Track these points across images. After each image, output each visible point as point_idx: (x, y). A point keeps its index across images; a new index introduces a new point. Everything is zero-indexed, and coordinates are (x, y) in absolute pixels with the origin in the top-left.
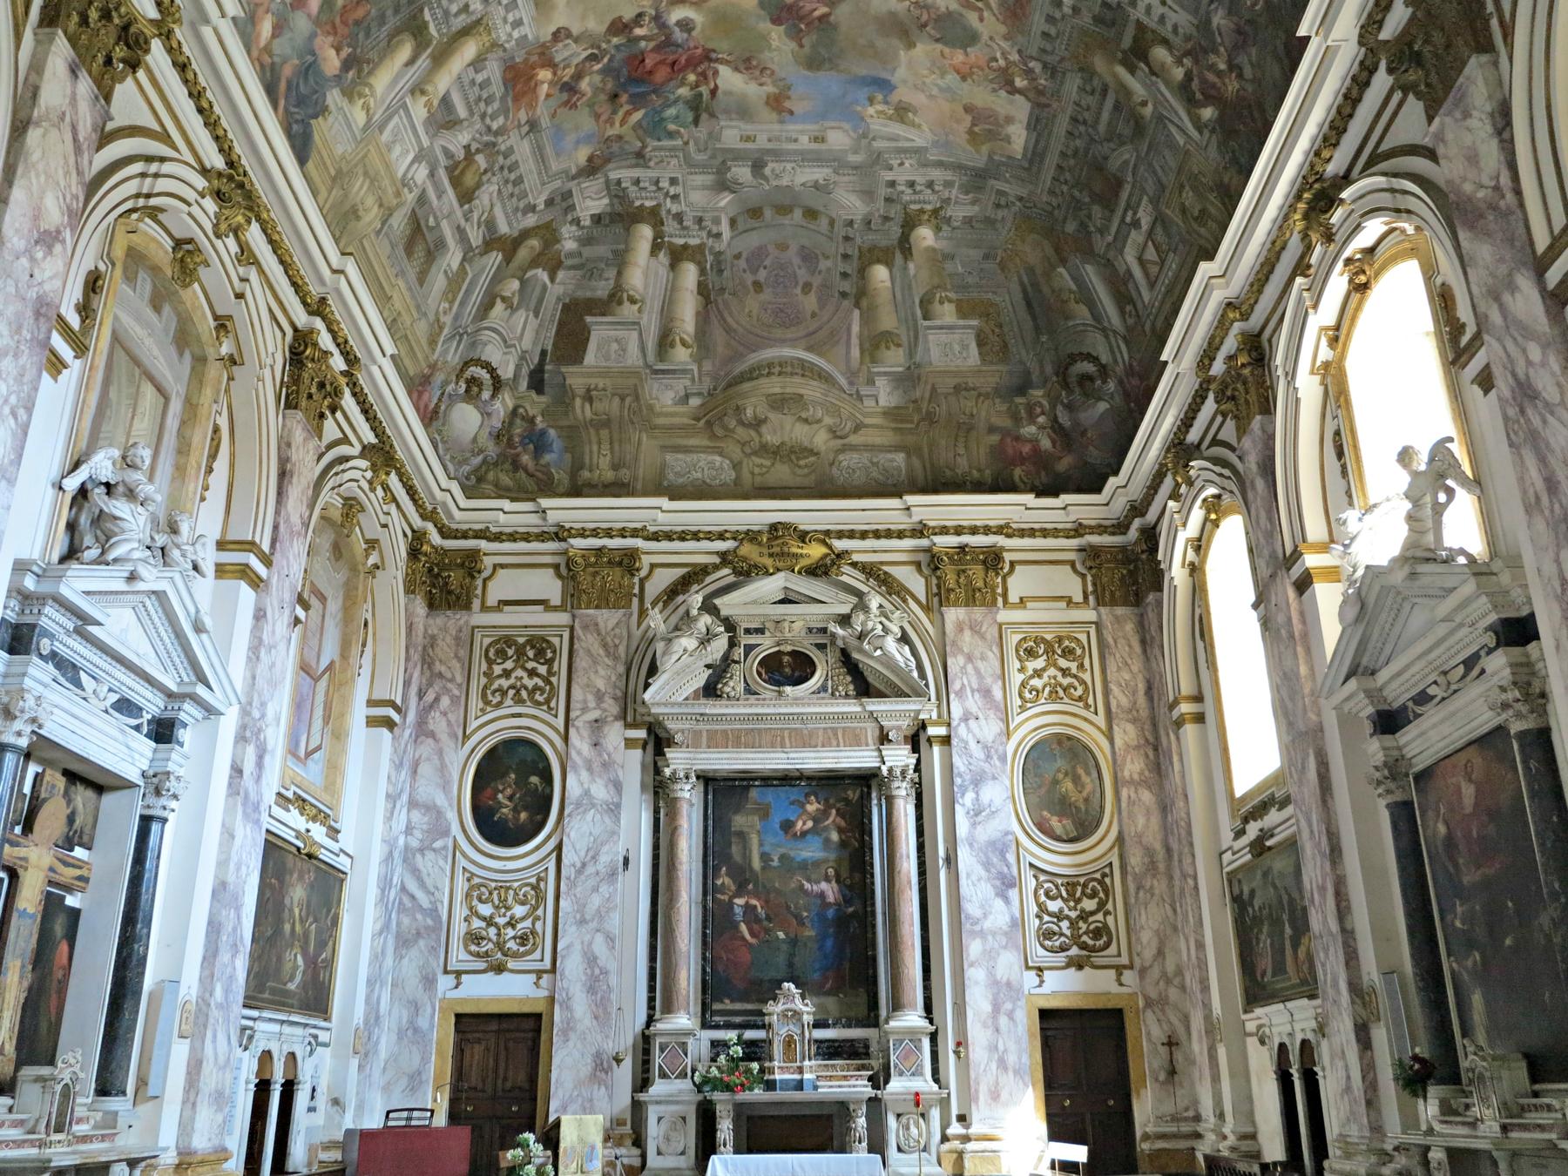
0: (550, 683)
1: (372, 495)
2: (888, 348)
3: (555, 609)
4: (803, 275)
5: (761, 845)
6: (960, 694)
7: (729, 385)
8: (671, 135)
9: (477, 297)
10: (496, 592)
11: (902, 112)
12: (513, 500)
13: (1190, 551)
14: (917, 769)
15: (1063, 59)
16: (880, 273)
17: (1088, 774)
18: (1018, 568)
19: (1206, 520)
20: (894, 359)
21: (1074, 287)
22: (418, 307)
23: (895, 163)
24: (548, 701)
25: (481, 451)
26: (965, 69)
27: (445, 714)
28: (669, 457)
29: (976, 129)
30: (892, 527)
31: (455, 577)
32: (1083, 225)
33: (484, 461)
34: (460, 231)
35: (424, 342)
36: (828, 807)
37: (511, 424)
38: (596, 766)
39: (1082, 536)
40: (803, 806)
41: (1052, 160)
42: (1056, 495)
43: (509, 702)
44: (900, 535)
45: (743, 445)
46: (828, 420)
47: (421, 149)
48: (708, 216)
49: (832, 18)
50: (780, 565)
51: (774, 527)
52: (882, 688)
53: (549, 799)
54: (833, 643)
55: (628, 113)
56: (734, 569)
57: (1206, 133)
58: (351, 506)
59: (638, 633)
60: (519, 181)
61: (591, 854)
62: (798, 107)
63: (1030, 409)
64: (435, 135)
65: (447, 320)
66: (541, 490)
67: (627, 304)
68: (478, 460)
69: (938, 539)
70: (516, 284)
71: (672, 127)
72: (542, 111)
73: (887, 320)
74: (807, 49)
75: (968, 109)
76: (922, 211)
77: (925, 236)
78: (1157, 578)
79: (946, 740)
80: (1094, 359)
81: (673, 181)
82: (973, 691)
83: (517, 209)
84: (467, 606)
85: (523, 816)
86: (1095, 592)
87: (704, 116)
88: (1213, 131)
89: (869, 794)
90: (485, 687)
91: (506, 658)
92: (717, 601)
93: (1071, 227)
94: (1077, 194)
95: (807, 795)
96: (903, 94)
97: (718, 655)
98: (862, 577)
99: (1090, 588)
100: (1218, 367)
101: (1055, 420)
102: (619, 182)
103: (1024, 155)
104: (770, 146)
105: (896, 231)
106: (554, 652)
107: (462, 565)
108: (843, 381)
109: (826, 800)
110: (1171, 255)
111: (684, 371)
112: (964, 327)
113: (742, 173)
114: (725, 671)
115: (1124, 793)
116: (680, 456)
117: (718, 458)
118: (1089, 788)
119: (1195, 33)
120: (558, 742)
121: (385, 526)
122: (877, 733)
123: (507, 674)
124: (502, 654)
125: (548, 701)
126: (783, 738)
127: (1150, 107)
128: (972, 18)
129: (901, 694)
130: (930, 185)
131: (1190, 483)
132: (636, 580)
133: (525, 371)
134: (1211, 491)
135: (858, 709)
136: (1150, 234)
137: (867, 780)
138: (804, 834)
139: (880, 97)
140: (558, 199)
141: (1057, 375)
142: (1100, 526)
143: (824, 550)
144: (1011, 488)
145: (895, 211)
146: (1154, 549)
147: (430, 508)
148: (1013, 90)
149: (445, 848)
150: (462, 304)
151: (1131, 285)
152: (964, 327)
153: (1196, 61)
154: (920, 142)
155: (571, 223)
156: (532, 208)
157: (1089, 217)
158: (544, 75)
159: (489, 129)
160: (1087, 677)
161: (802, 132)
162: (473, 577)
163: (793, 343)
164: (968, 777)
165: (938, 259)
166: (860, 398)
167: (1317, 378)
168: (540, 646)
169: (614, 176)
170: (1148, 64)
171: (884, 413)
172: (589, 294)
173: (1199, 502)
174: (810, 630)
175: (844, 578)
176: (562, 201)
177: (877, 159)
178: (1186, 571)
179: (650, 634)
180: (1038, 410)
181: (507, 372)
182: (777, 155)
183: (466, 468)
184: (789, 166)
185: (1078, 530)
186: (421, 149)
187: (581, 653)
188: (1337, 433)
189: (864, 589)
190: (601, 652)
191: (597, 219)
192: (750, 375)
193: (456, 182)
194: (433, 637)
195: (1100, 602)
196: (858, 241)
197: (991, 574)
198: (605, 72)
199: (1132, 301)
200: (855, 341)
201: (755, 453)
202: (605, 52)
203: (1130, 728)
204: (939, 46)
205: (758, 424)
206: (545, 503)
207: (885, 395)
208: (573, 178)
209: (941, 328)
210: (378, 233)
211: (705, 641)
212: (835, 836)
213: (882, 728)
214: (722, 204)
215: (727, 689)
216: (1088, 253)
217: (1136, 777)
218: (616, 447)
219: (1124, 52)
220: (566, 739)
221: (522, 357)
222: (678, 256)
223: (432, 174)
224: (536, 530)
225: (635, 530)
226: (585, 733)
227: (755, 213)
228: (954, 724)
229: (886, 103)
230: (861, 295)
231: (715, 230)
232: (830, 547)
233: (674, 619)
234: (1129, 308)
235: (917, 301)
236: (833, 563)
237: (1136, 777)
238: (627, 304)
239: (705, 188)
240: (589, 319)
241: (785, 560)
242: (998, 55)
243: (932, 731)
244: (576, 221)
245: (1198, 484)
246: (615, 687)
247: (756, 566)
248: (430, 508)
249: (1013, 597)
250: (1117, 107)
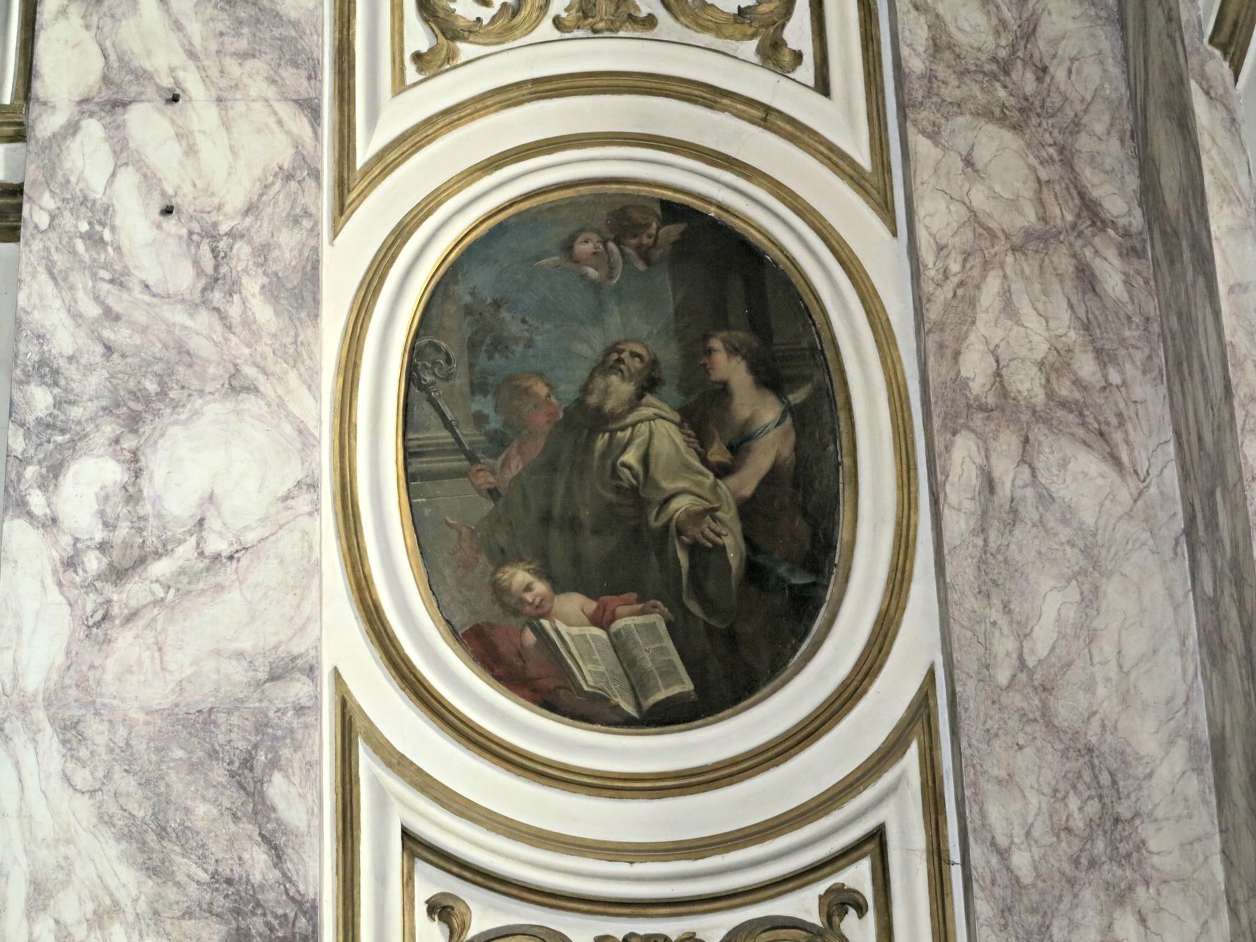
115: (963, 455)
203: (997, 147)
217: (1027, 383)
237: (1027, 383)
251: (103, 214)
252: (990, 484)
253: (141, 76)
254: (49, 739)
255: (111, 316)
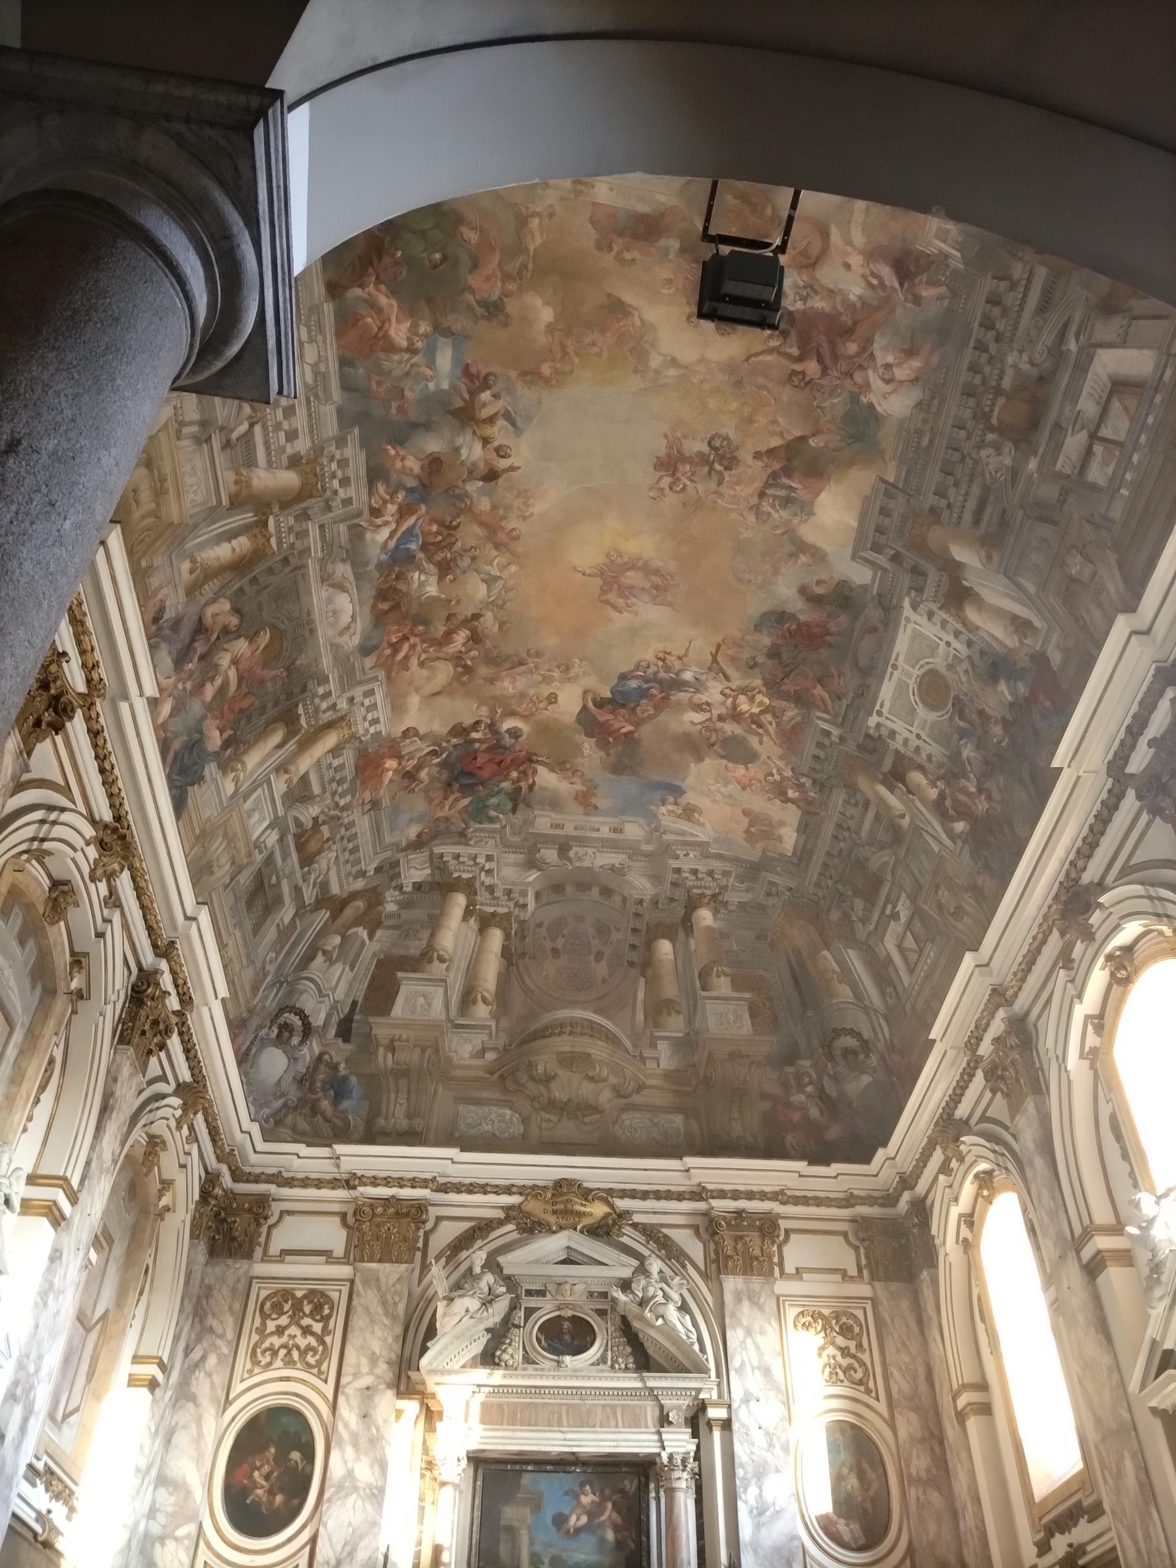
0: (322, 1342)
1: (177, 1134)
2: (669, 1015)
3: (338, 1262)
4: (596, 944)
5: (532, 1543)
6: (740, 1371)
7: (524, 1042)
8: (491, 820)
9: (302, 948)
10: (281, 1239)
11: (689, 813)
12: (309, 1145)
13: (963, 1226)
14: (697, 1457)
15: (830, 777)
16: (665, 947)
17: (875, 1470)
18: (793, 1236)
19: (978, 1195)
20: (675, 1026)
21: (837, 969)
22: (248, 955)
23: (681, 853)
24: (319, 1364)
25: (283, 1095)
26: (746, 781)
27: (209, 1375)
28: (462, 1108)
29: (752, 829)
30: (673, 1188)
31: (240, 1223)
32: (846, 915)
33: (285, 1105)
34: (297, 891)
35: (248, 987)
36: (604, 1499)
37: (315, 1069)
38: (363, 1441)
39: (853, 1206)
40: (577, 1497)
41: (818, 858)
42: (827, 1163)
43: (278, 1363)
44: (680, 1197)
45: (533, 1100)
46: (613, 1080)
47: (276, 817)
48: (517, 889)
49: (636, 735)
50: (563, 1222)
51: (559, 1184)
52: (662, 1361)
53: (308, 1479)
54: (613, 1309)
55: (457, 800)
56: (518, 1225)
57: (960, 843)
58: (156, 1144)
59: (417, 1291)
60: (355, 850)
61: (348, 1549)
62: (602, 803)
63: (799, 1077)
64: (290, 807)
65: (272, 968)
66: (336, 1136)
67: (436, 963)
68: (278, 1104)
69: (715, 1203)
70: (337, 940)
71: (492, 813)
72: (384, 794)
73: (670, 990)
74: (612, 758)
75: (746, 813)
76: (703, 895)
77: (705, 917)
78: (930, 1256)
79: (727, 1425)
80: (858, 1035)
81: (489, 858)
82: (753, 1369)
83: (350, 874)
84: (249, 1256)
85: (279, 1499)
86: (868, 1265)
87: (521, 806)
88: (965, 841)
89: (647, 1485)
90: (256, 1346)
91: (282, 1313)
92: (501, 1259)
93: (835, 916)
94: (840, 887)
95: (582, 1485)
96: (690, 798)
97: (498, 1319)
98: (642, 1239)
99: (864, 1262)
100: (985, 1048)
101: (822, 1090)
102: (441, 856)
103: (794, 853)
104: (575, 833)
105: (680, 911)
106: (332, 1309)
107: (250, 1210)
108: (627, 1043)
109: (602, 1491)
110: (929, 945)
111: (483, 1027)
112: (738, 999)
113: (550, 854)
114: (505, 1336)
116: (472, 1108)
117: (508, 1112)
118: (875, 1486)
119: (946, 760)
120: (325, 1411)
121: (183, 1166)
122: (657, 1413)
123: (280, 1331)
124: (278, 1309)
125: (319, 1364)
126: (560, 1416)
127: (907, 820)
128: (754, 741)
129: (681, 1369)
130: (711, 873)
131: (961, 1160)
132: (421, 1233)
133: (335, 1020)
134: (983, 1166)
135: (639, 1385)
136: (908, 926)
137: (644, 1470)
138: (578, 1531)
139: (671, 799)
140: (386, 867)
141: (823, 1047)
142: (870, 1197)
143: (606, 1209)
144: (784, 1155)
145: (679, 894)
146: (925, 1224)
147: (227, 1149)
148: (786, 800)
149: (187, 1537)
150: (288, 954)
151: (891, 970)
152: (738, 999)
153: (948, 784)
154: (703, 838)
155: (394, 888)
156: (363, 874)
157: (852, 909)
158: (391, 764)
159: (337, 804)
160: (865, 1357)
161: (604, 823)
162: (259, 1225)
163: (584, 1005)
164: (750, 1469)
165: (716, 937)
166: (643, 1060)
167: (1087, 1063)
168: (319, 1302)
169: (437, 850)
170: (905, 785)
171: (665, 1076)
172: (402, 952)
173: (970, 1177)
174: (591, 1294)
175: (625, 1240)
176: (390, 870)
177: (666, 850)
178: (961, 1248)
179: (430, 1292)
180: (807, 1080)
181: (318, 1020)
182: (581, 841)
183: (267, 1111)
184: (590, 851)
185: (849, 1201)
186: (276, 817)
187: (359, 1309)
188: (1113, 1119)
189: (646, 1252)
190: (380, 1310)
191: (418, 887)
192: (545, 1033)
193: (300, 848)
194: (210, 1288)
195: (873, 1277)
196: (647, 917)
197: (767, 1242)
198: (443, 765)
199: (892, 984)
200: (640, 1007)
201: (543, 1109)
202: (443, 750)
203: (913, 1417)
204: (724, 762)
205: (548, 1079)
206: (340, 1149)
207: (665, 1058)
208: (402, 850)
209: (718, 998)
210: (226, 887)
211: (487, 1303)
212: (610, 1536)
213: (662, 1407)
214: (531, 879)
215: (506, 1357)
216: (851, 939)
217: (923, 1474)
218: (413, 1096)
219: (884, 774)
220: (334, 1407)
221: (334, 1007)
222: (486, 923)
223: (281, 840)
224: (328, 1177)
225: (426, 1180)
226: (355, 1402)
227: (558, 888)
228: (735, 1406)
229: (676, 804)
230: (646, 964)
231: (521, 901)
232: (612, 1206)
233: (455, 1276)
234: (889, 990)
235: (697, 975)
236: (614, 1221)
237: (923, 1474)
238: (436, 963)
239: (516, 865)
240: (400, 974)
241: (568, 1218)
242: (774, 771)
243: (714, 1413)
244: (400, 888)
245: (969, 1159)
246: (391, 1349)
247: (540, 1223)
248: (227, 1149)
249: (790, 1268)
250: (878, 818)
251: (748, 1428)
252: (918, 1499)
253: (751, 1394)
254: (752, 1553)
255: (752, 1453)
